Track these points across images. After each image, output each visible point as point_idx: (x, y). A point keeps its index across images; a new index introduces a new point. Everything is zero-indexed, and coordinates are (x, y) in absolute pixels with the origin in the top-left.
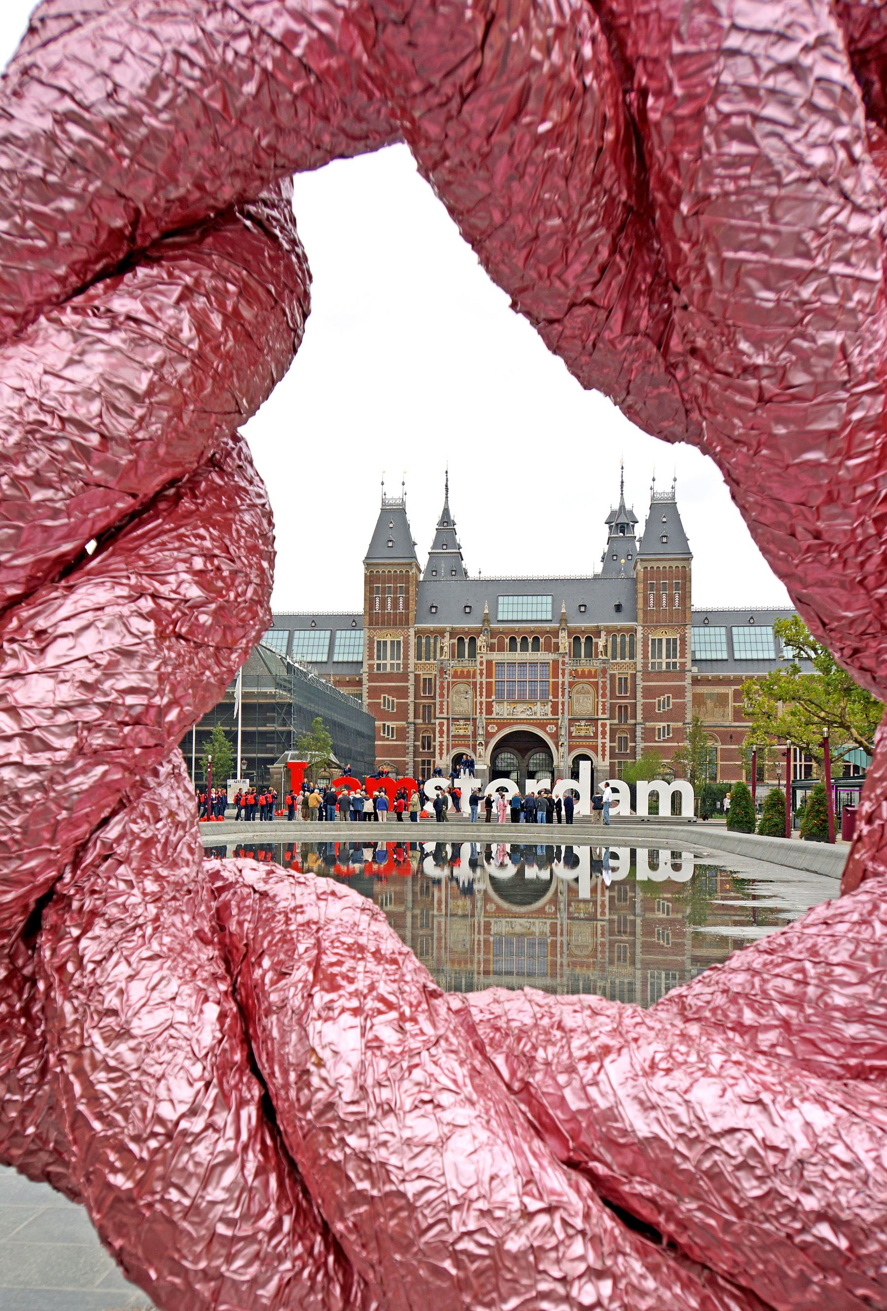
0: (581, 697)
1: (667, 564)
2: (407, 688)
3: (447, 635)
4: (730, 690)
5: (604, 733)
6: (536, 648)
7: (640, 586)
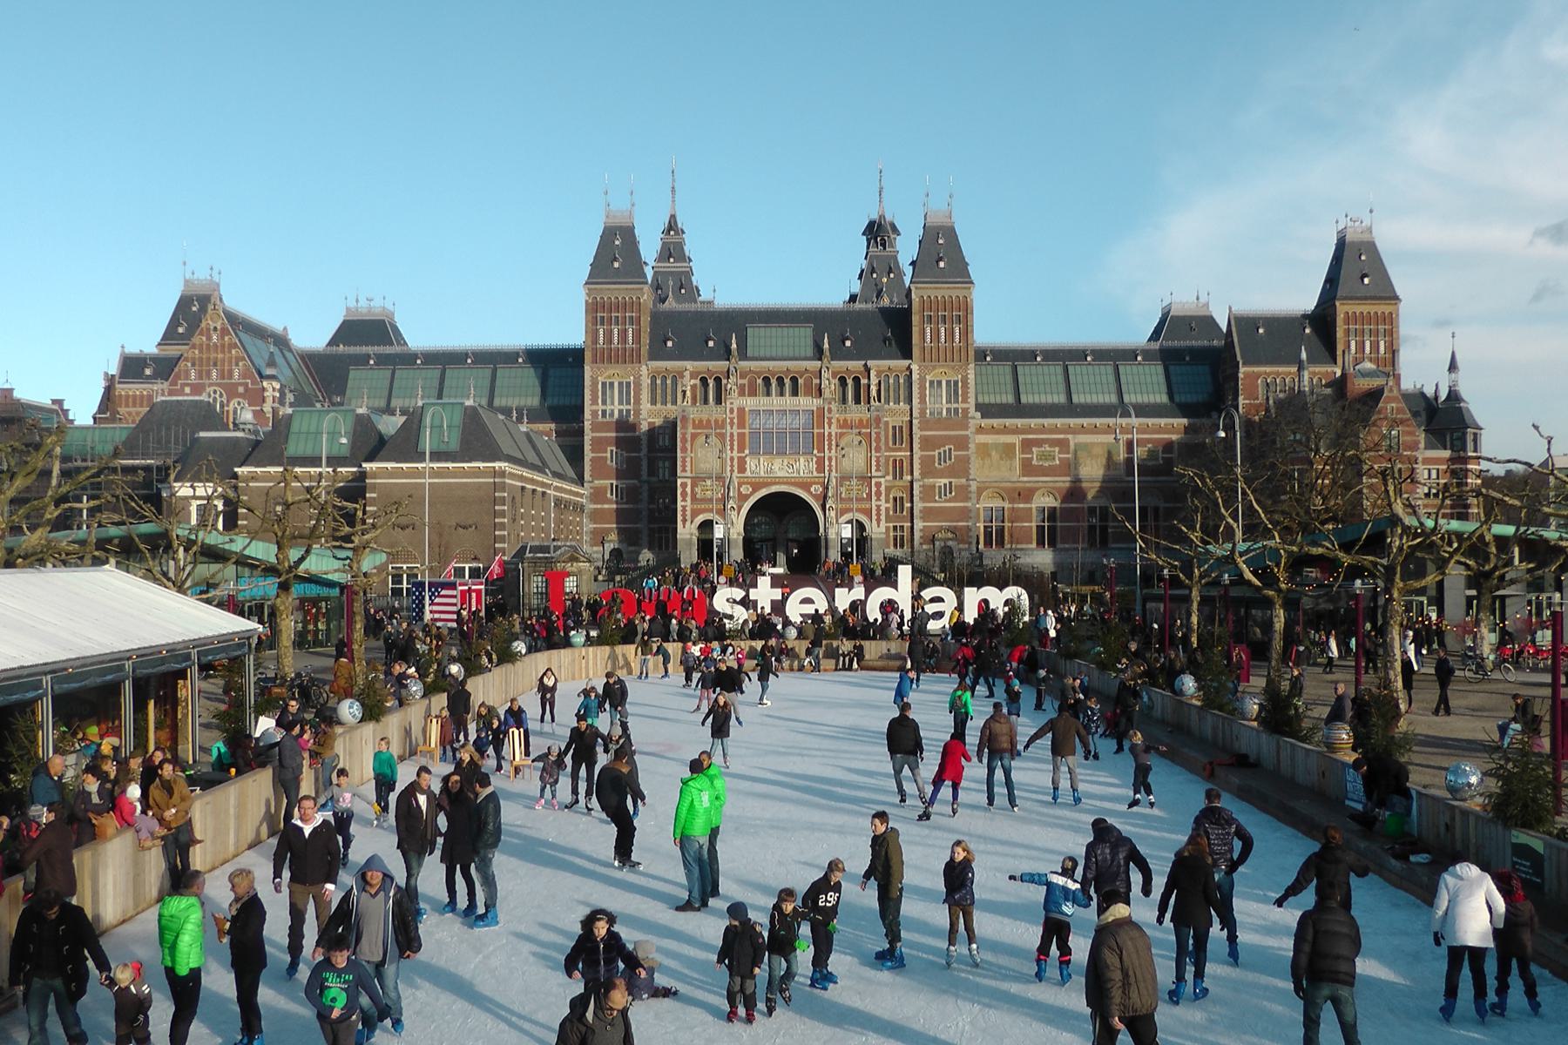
4: (1015, 439)
7: (915, 319)
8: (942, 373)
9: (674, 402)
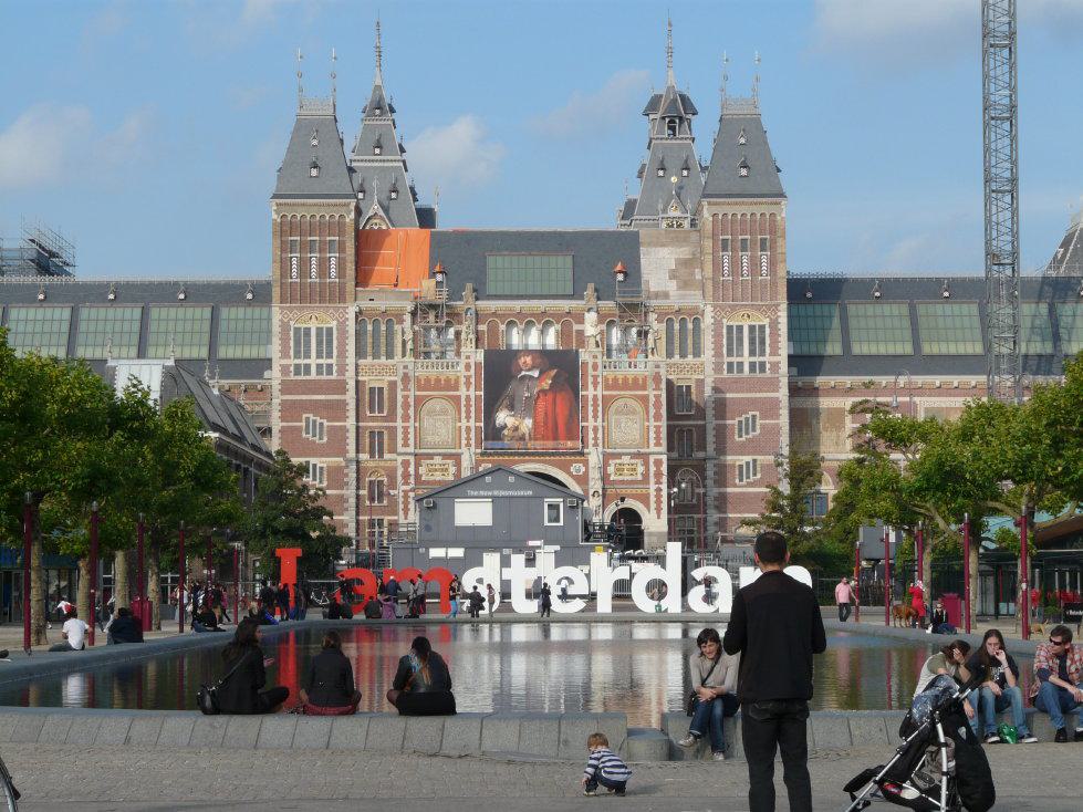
0: (623, 418)
1: (748, 210)
2: (344, 403)
3: (408, 318)
5: (658, 474)
9: (390, 355)
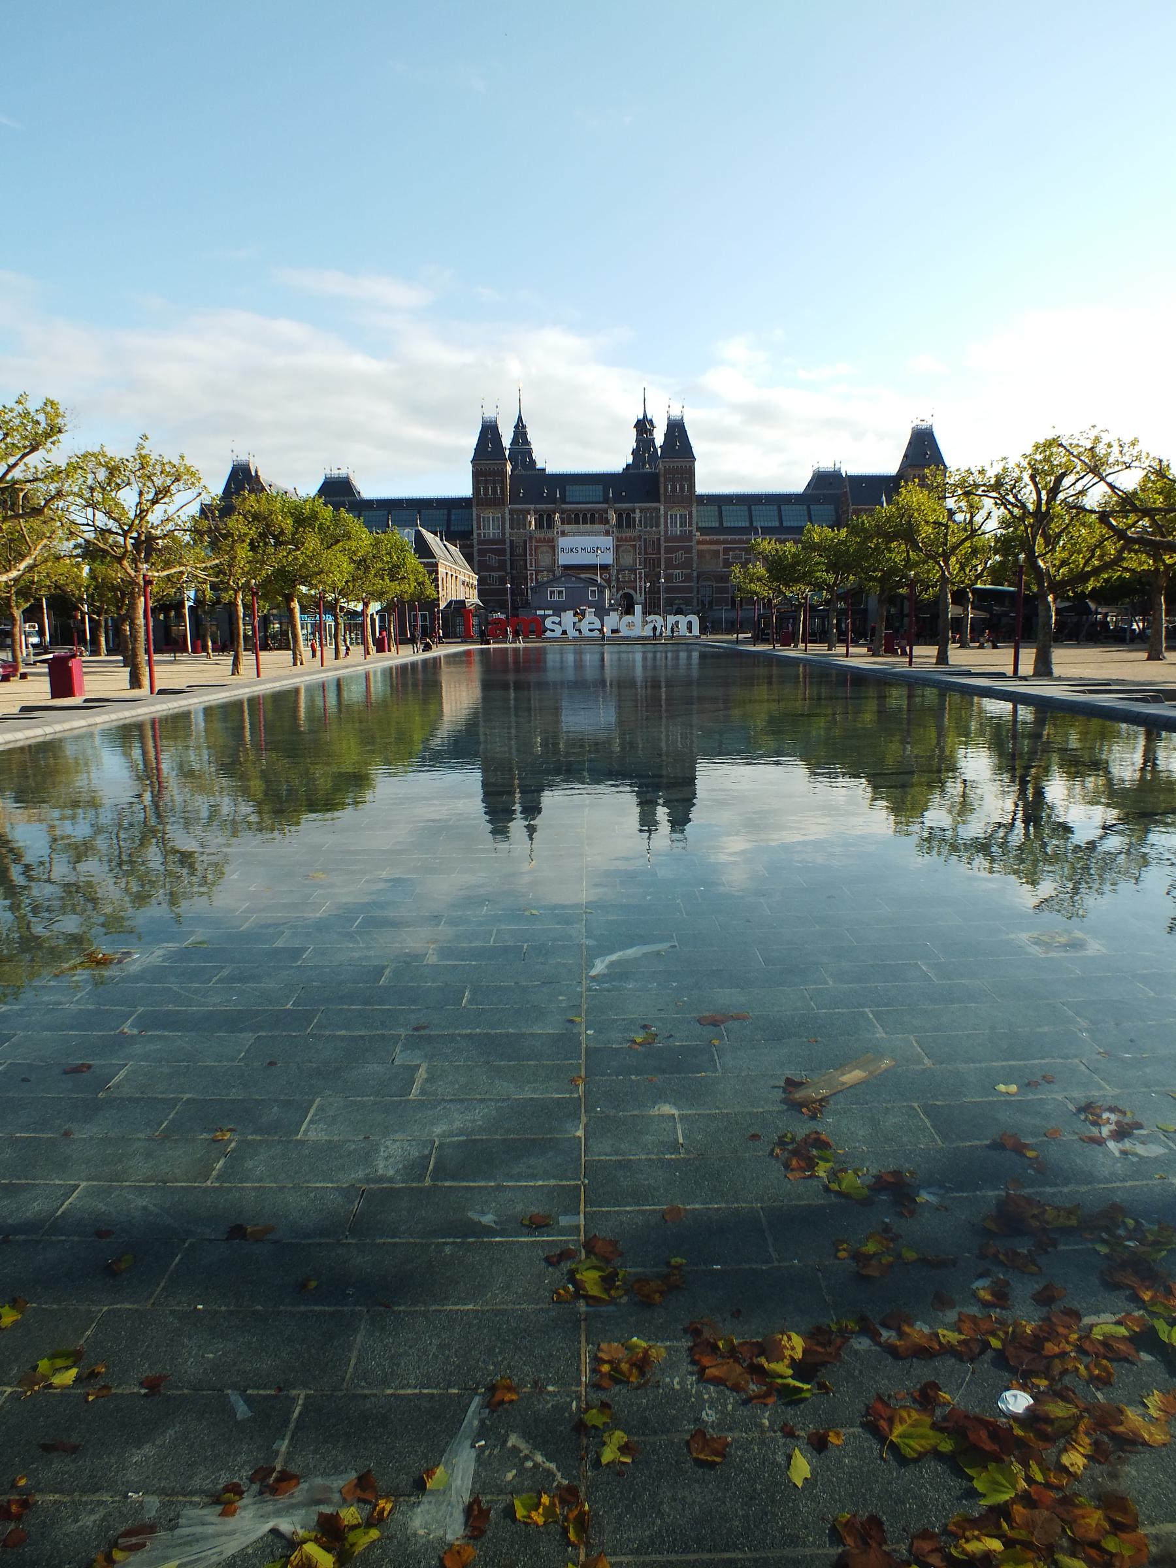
4: (721, 547)
5: (640, 578)
6: (593, 522)
7: (662, 479)
8: (678, 512)
